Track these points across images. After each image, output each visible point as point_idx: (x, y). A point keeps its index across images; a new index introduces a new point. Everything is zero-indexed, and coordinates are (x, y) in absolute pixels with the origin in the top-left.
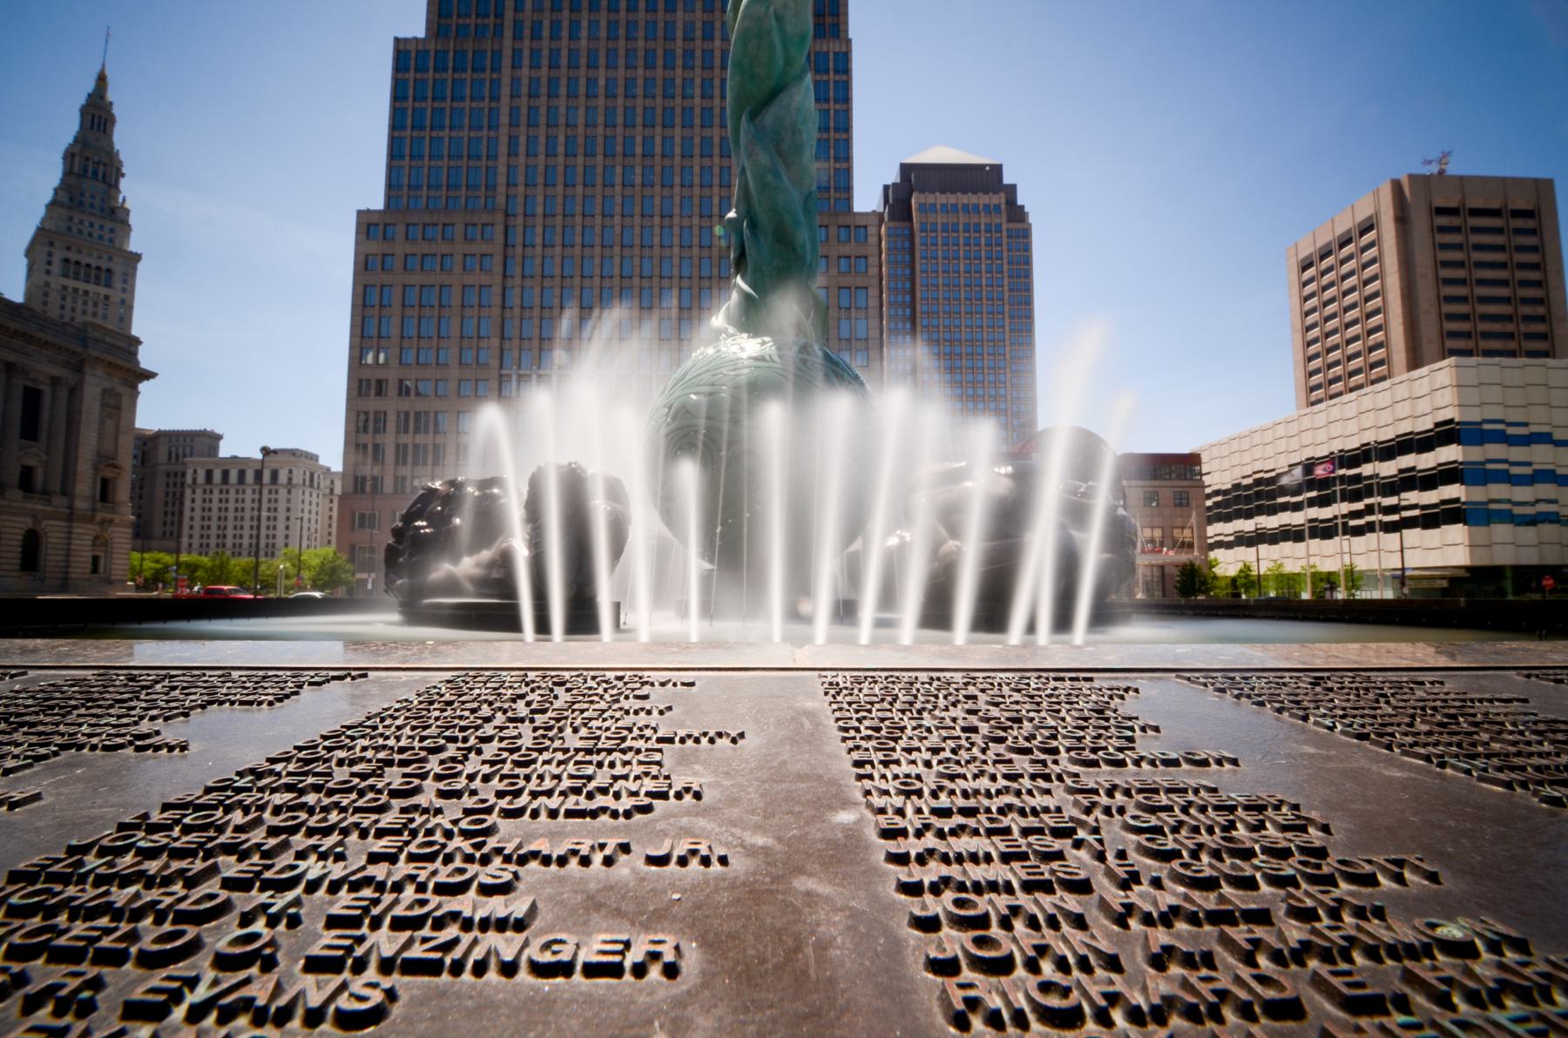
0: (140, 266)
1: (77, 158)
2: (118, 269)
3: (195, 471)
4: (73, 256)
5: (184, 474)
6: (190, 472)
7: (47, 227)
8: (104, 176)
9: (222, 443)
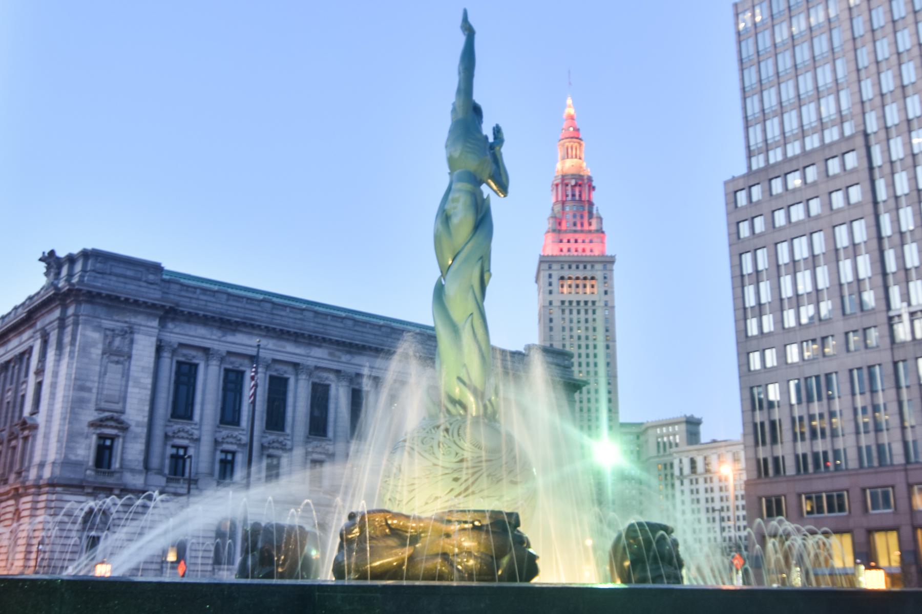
0: (616, 267)
1: (560, 187)
2: (599, 275)
3: (681, 461)
4: (566, 273)
5: (672, 465)
6: (676, 462)
7: (549, 252)
8: (580, 196)
9: (702, 428)
